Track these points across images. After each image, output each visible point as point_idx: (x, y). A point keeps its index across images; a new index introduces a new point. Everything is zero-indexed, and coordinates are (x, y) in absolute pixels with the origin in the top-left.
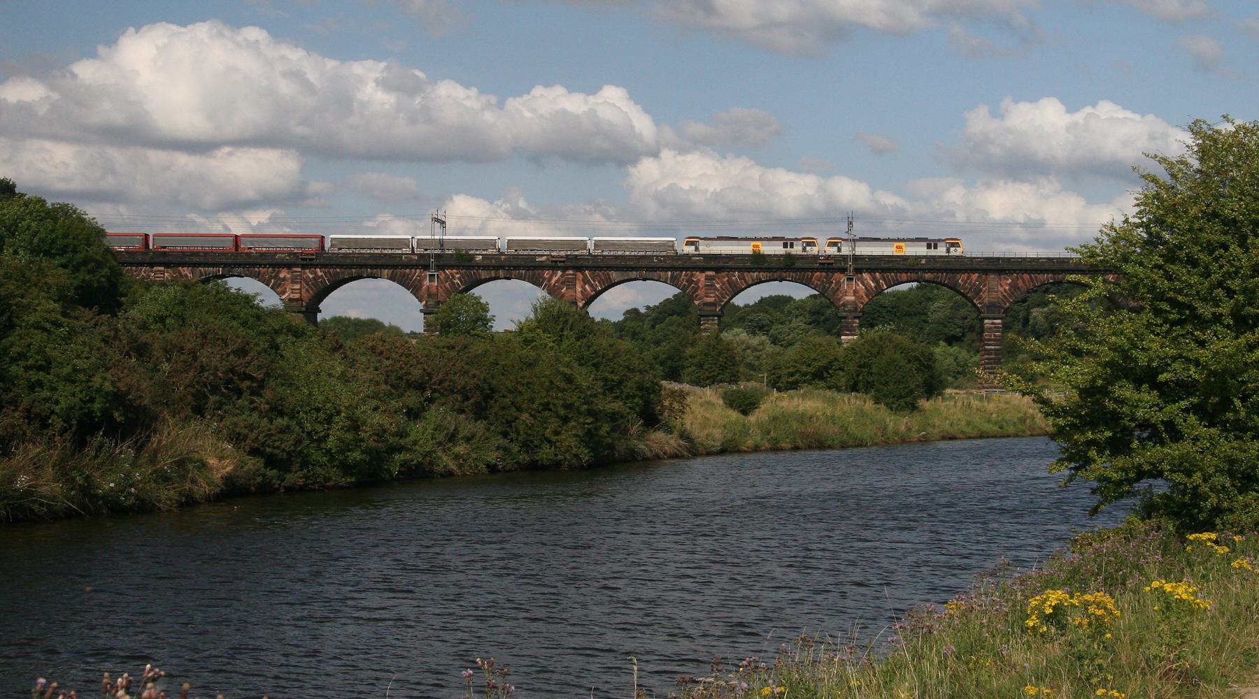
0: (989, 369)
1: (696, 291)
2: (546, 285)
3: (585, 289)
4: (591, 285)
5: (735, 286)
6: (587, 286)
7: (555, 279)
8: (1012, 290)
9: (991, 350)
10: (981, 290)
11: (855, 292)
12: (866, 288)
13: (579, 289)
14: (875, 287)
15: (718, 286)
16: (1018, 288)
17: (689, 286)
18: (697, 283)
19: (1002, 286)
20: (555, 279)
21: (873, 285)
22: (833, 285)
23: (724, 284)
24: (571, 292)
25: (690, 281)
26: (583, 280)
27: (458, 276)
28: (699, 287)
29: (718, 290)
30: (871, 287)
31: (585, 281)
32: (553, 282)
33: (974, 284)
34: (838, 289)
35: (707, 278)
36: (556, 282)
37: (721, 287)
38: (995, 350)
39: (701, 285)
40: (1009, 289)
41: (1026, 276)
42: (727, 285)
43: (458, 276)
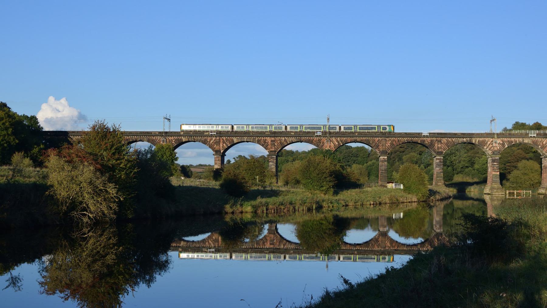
0: (382, 176)
1: (267, 146)
2: (208, 144)
3: (224, 146)
4: (226, 144)
5: (283, 144)
6: (224, 144)
7: (212, 141)
12: (334, 145)
13: (221, 146)
14: (338, 144)
15: (276, 144)
16: (394, 145)
17: (264, 144)
18: (267, 143)
20: (212, 141)
21: (337, 143)
22: (321, 144)
23: (278, 143)
24: (218, 147)
26: (223, 142)
27: (174, 140)
28: (268, 144)
29: (276, 146)
30: (336, 145)
31: (224, 142)
32: (211, 142)
33: (376, 143)
34: (323, 145)
35: (272, 141)
36: (212, 143)
37: (277, 144)
38: (384, 169)
40: (390, 145)
42: (279, 143)
43: (174, 140)
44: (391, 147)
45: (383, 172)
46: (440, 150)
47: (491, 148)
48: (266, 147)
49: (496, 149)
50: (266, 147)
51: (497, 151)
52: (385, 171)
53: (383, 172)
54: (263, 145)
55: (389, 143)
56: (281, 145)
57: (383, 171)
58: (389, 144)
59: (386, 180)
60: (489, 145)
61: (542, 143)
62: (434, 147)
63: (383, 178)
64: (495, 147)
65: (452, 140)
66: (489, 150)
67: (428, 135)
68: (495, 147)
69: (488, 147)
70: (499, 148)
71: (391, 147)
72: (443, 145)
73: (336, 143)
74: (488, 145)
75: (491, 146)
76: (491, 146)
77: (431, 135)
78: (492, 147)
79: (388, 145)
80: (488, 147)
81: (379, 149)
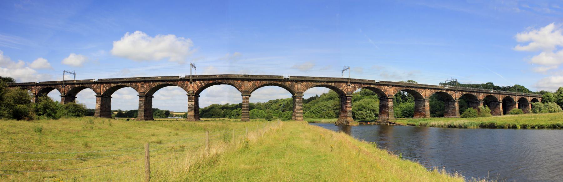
0: (243, 113)
4: (105, 88)
5: (151, 86)
6: (104, 88)
8: (253, 86)
9: (245, 106)
10: (242, 86)
11: (193, 87)
12: (197, 86)
13: (102, 89)
14: (201, 85)
15: (145, 87)
16: (256, 85)
17: (136, 87)
18: (138, 86)
19: (249, 84)
21: (200, 84)
22: (185, 85)
24: (99, 90)
25: (136, 85)
26: (103, 86)
31: (104, 87)
33: (239, 84)
34: (187, 86)
38: (246, 106)
39: (139, 87)
40: (252, 86)
41: (259, 82)
42: (148, 86)
44: (253, 87)
45: (245, 108)
46: (300, 91)
47: (345, 89)
48: (137, 89)
49: (349, 90)
50: (137, 89)
51: (350, 92)
52: (246, 108)
53: (245, 108)
54: (134, 88)
55: (251, 84)
56: (150, 87)
57: (245, 108)
58: (251, 85)
59: (247, 116)
60: (344, 87)
61: (384, 88)
62: (294, 88)
63: (244, 114)
64: (349, 89)
65: (312, 84)
66: (344, 91)
67: (289, 77)
68: (349, 89)
69: (343, 88)
70: (352, 90)
71: (253, 87)
72: (303, 87)
73: (199, 84)
74: (343, 87)
75: (345, 88)
76: (345, 88)
77: (292, 78)
78: (346, 89)
79: (251, 86)
80: (343, 88)
81: (241, 89)
